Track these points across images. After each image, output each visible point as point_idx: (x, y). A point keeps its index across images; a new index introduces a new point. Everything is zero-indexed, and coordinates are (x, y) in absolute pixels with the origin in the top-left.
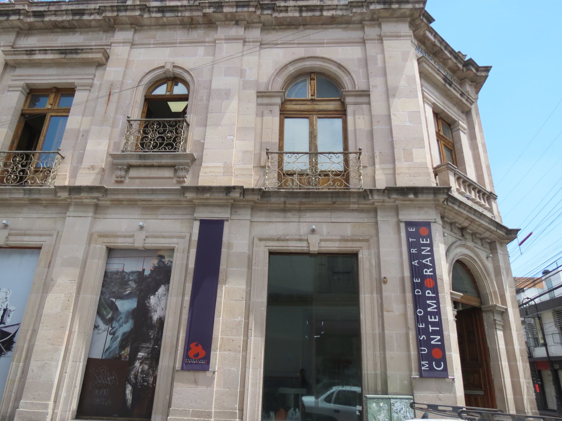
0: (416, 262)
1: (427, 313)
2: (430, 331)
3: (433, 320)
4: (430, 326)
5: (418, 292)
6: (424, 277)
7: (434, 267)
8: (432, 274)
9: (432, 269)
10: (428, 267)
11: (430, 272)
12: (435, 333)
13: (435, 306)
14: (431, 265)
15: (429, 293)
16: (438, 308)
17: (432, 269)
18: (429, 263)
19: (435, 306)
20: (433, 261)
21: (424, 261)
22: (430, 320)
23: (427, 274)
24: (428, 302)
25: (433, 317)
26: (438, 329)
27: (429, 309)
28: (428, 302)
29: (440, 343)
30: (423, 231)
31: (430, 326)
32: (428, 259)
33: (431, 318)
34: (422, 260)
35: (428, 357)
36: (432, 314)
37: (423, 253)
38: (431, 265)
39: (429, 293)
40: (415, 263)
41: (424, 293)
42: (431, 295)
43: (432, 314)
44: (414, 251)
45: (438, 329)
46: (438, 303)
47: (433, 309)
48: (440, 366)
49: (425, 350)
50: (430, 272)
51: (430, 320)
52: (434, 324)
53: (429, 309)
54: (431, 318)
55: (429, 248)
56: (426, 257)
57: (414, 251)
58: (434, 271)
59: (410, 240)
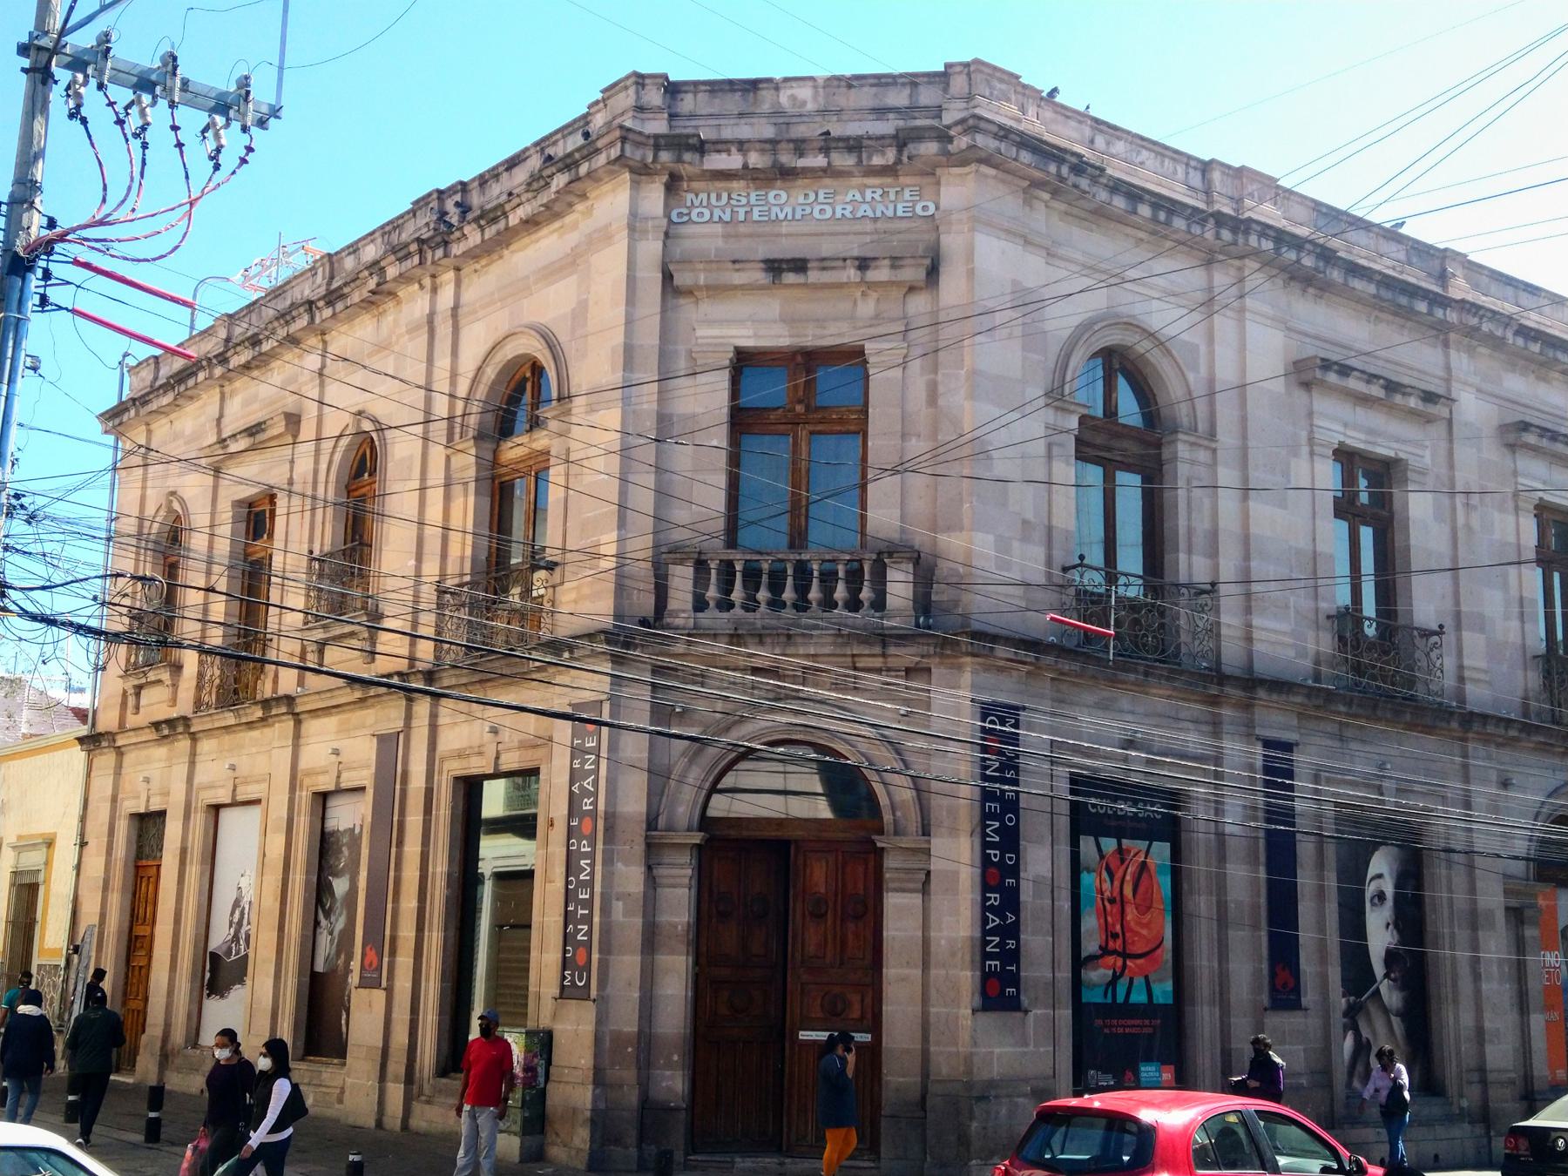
5: (1010, 859)
7: (985, 908)
10: (992, 909)
16: (984, 827)
20: (985, 921)
27: (997, 824)
28: (997, 839)
32: (991, 925)
37: (998, 939)
39: (995, 855)
40: (1011, 918)
42: (992, 852)
46: (984, 835)
53: (997, 824)
55: (988, 949)
56: (992, 932)
58: (985, 899)
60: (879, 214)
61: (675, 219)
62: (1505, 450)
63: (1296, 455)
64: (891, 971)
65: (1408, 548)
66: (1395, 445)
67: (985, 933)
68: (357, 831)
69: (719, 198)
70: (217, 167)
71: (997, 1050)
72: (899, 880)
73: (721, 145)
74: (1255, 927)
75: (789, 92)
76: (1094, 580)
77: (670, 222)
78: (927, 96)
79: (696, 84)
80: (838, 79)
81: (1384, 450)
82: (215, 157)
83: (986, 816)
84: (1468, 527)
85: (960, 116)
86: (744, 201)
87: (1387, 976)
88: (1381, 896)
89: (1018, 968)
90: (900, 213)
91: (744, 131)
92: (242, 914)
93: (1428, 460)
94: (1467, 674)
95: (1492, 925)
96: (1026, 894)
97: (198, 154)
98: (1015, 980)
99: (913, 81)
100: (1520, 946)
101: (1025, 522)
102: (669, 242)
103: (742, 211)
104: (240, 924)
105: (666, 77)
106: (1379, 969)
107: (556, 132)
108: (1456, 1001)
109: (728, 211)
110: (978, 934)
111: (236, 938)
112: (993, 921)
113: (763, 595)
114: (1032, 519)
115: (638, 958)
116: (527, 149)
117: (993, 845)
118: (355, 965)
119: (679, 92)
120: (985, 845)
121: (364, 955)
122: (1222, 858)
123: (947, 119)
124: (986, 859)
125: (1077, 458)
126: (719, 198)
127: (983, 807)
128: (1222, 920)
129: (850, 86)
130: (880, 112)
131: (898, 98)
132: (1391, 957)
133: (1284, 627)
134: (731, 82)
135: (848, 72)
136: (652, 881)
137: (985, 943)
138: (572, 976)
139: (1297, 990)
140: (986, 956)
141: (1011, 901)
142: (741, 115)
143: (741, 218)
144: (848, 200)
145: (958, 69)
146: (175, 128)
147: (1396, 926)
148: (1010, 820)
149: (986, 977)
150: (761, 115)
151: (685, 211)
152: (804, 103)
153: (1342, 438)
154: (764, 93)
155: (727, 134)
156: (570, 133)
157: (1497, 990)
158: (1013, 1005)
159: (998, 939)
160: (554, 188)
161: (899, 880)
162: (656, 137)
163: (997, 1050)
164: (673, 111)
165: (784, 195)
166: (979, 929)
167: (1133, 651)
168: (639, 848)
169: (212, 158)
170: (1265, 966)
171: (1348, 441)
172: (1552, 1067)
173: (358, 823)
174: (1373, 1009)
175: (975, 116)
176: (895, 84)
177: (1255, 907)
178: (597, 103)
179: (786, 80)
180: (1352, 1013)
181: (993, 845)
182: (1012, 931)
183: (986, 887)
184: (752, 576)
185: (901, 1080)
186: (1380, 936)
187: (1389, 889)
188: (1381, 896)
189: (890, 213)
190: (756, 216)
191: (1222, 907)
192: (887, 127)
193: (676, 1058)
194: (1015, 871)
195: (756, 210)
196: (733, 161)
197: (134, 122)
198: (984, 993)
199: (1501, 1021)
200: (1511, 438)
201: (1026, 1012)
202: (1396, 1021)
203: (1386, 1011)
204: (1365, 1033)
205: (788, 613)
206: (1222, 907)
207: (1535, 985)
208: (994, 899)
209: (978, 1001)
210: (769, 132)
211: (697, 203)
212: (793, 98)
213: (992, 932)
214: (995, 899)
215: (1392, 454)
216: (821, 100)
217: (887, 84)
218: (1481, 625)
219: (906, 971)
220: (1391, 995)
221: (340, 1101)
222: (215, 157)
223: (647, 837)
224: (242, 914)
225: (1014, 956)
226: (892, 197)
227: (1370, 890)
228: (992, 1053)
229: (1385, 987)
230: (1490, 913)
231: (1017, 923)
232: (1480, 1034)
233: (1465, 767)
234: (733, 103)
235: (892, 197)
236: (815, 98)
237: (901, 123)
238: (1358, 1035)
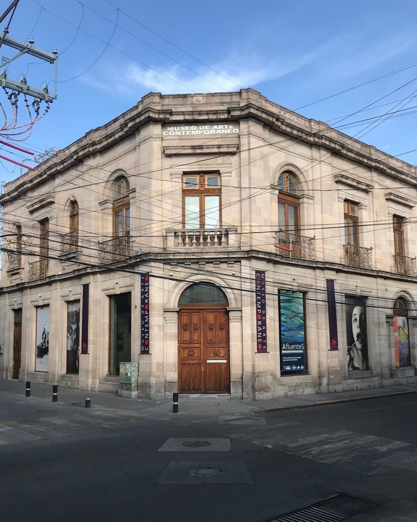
10: (259, 326)
24: (260, 307)
28: (260, 307)
37: (261, 334)
40: (264, 328)
41: (261, 311)
46: (257, 306)
60: (223, 133)
61: (164, 134)
63: (334, 201)
64: (232, 343)
66: (359, 199)
68: (78, 311)
69: (177, 129)
70: (38, 114)
73: (178, 113)
75: (196, 98)
77: (163, 135)
78: (236, 99)
79: (169, 96)
80: (211, 94)
82: (37, 111)
83: (257, 301)
85: (245, 104)
86: (184, 129)
87: (357, 340)
88: (356, 320)
90: (229, 132)
91: (183, 109)
92: (46, 335)
93: (367, 203)
96: (268, 322)
97: (32, 110)
98: (265, 344)
99: (231, 94)
100: (389, 331)
101: (265, 220)
102: (163, 141)
103: (183, 132)
104: (45, 338)
105: (161, 94)
106: (355, 338)
107: (128, 111)
109: (180, 132)
111: (44, 342)
113: (194, 241)
116: (119, 116)
118: (80, 348)
119: (164, 98)
120: (257, 308)
121: (82, 345)
123: (242, 105)
124: (257, 313)
126: (177, 129)
129: (213, 96)
130: (222, 103)
131: (227, 99)
132: (358, 335)
134: (179, 95)
135: (212, 92)
138: (144, 348)
142: (182, 105)
143: (184, 134)
144: (214, 128)
145: (244, 91)
146: (26, 101)
147: (360, 327)
149: (258, 343)
150: (188, 105)
151: (167, 132)
152: (200, 101)
154: (189, 98)
155: (179, 110)
156: (132, 111)
157: (384, 343)
158: (265, 351)
159: (261, 334)
160: (129, 126)
162: (159, 110)
164: (163, 104)
165: (195, 127)
169: (36, 111)
170: (329, 339)
171: (347, 198)
172: (396, 361)
173: (78, 309)
174: (354, 349)
175: (250, 103)
176: (226, 95)
178: (140, 102)
179: (195, 94)
180: (349, 350)
183: (258, 320)
184: (191, 237)
186: (356, 330)
187: (358, 319)
188: (356, 320)
189: (226, 132)
190: (188, 134)
192: (225, 108)
193: (174, 369)
194: (265, 315)
195: (188, 132)
196: (181, 118)
197: (13, 100)
199: (385, 350)
202: (360, 352)
204: (352, 355)
205: (201, 246)
207: (393, 341)
210: (191, 109)
211: (170, 130)
212: (197, 100)
216: (205, 100)
217: (224, 95)
219: (236, 343)
220: (359, 345)
221: (78, 384)
222: (37, 111)
224: (46, 335)
225: (265, 338)
226: (226, 128)
230: (382, 323)
231: (266, 329)
234: (180, 101)
235: (226, 128)
236: (203, 99)
237: (228, 106)
238: (350, 356)
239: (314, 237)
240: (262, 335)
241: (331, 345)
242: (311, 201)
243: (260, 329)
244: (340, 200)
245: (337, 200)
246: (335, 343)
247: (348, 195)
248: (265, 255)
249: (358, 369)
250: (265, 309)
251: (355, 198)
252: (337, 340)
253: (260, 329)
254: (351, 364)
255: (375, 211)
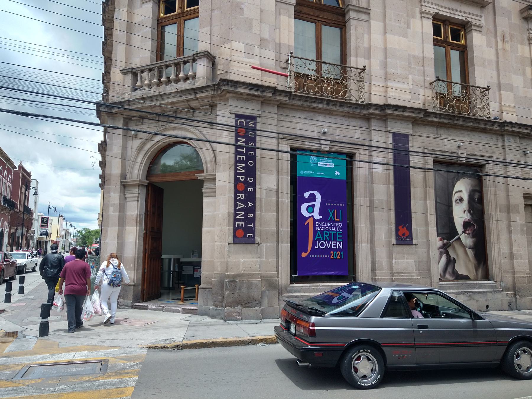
0: (250, 206)
1: (246, 162)
2: (244, 148)
3: (241, 157)
4: (244, 152)
5: (251, 180)
6: (245, 192)
7: (236, 200)
8: (237, 195)
9: (237, 198)
10: (240, 200)
11: (239, 196)
12: (242, 147)
13: (238, 168)
14: (237, 202)
15: (242, 178)
16: (236, 166)
17: (237, 198)
18: (239, 204)
19: (238, 168)
20: (236, 205)
21: (243, 206)
22: (244, 157)
23: (242, 195)
24: (244, 171)
25: (241, 159)
26: (238, 150)
27: (244, 165)
28: (244, 171)
29: (238, 139)
30: (240, 233)
31: (244, 152)
32: (239, 207)
33: (243, 158)
34: (244, 207)
35: (248, 129)
36: (241, 161)
37: (243, 213)
38: (237, 202)
39: (242, 178)
40: (250, 204)
42: (241, 177)
43: (241, 161)
44: (250, 215)
45: (238, 150)
46: (236, 169)
47: (241, 140)
48: (240, 122)
49: (251, 134)
50: (239, 196)
51: (244, 157)
52: (241, 153)
53: (244, 165)
54: (243, 158)
55: (237, 217)
56: (240, 210)
57: (250, 215)
58: (236, 196)
59: (252, 225)
62: (522, 20)
63: (413, 17)
65: (473, 58)
66: (465, 15)
67: (235, 210)
71: (242, 260)
72: (209, 192)
74: (389, 209)
76: (310, 70)
81: (460, 16)
83: (237, 162)
84: (504, 49)
87: (464, 232)
88: (461, 200)
89: (254, 226)
94: (504, 108)
95: (518, 212)
98: (253, 230)
106: (460, 229)
108: (499, 243)
110: (232, 211)
112: (240, 205)
114: (269, 39)
115: (117, 228)
117: (241, 174)
120: (236, 174)
122: (372, 183)
124: (237, 180)
125: (295, 18)
127: (236, 157)
128: (372, 207)
132: (466, 225)
133: (405, 86)
136: (124, 199)
137: (235, 215)
139: (411, 236)
140: (236, 220)
141: (251, 197)
147: (469, 212)
148: (251, 163)
153: (437, 11)
161: (209, 192)
163: (242, 260)
166: (233, 209)
167: (319, 93)
168: (118, 186)
170: (393, 226)
171: (440, 13)
174: (457, 245)
177: (388, 202)
181: (241, 174)
182: (253, 210)
183: (237, 191)
185: (207, 273)
187: (465, 197)
191: (371, 202)
193: (132, 265)
194: (253, 185)
198: (235, 236)
200: (525, 14)
201: (259, 244)
203: (464, 246)
204: (452, 255)
206: (371, 202)
208: (242, 196)
209: (231, 239)
213: (240, 210)
214: (242, 196)
215: (464, 19)
218: (510, 88)
220: (467, 240)
223: (121, 182)
227: (455, 197)
228: (239, 261)
229: (463, 237)
231: (254, 206)
232: (511, 256)
233: (504, 146)
239: (365, 67)
240: (245, 215)
241: (397, 235)
242: (364, 17)
243: (241, 206)
244: (423, 15)
245: (418, 15)
246: (407, 234)
247: (440, 9)
248: (250, 89)
249: (466, 278)
250: (254, 176)
251: (457, 13)
252: (410, 229)
253: (241, 206)
254: (450, 269)
255: (499, 33)
